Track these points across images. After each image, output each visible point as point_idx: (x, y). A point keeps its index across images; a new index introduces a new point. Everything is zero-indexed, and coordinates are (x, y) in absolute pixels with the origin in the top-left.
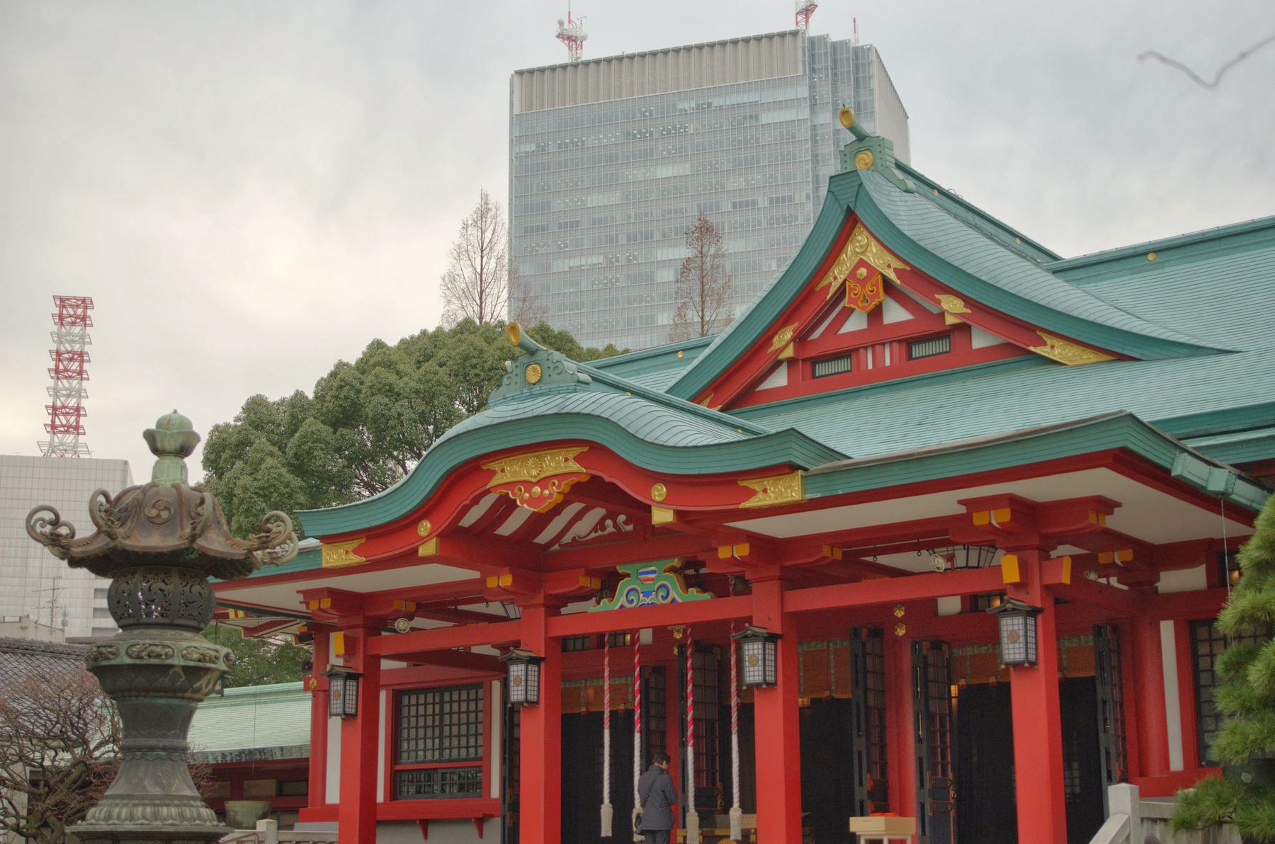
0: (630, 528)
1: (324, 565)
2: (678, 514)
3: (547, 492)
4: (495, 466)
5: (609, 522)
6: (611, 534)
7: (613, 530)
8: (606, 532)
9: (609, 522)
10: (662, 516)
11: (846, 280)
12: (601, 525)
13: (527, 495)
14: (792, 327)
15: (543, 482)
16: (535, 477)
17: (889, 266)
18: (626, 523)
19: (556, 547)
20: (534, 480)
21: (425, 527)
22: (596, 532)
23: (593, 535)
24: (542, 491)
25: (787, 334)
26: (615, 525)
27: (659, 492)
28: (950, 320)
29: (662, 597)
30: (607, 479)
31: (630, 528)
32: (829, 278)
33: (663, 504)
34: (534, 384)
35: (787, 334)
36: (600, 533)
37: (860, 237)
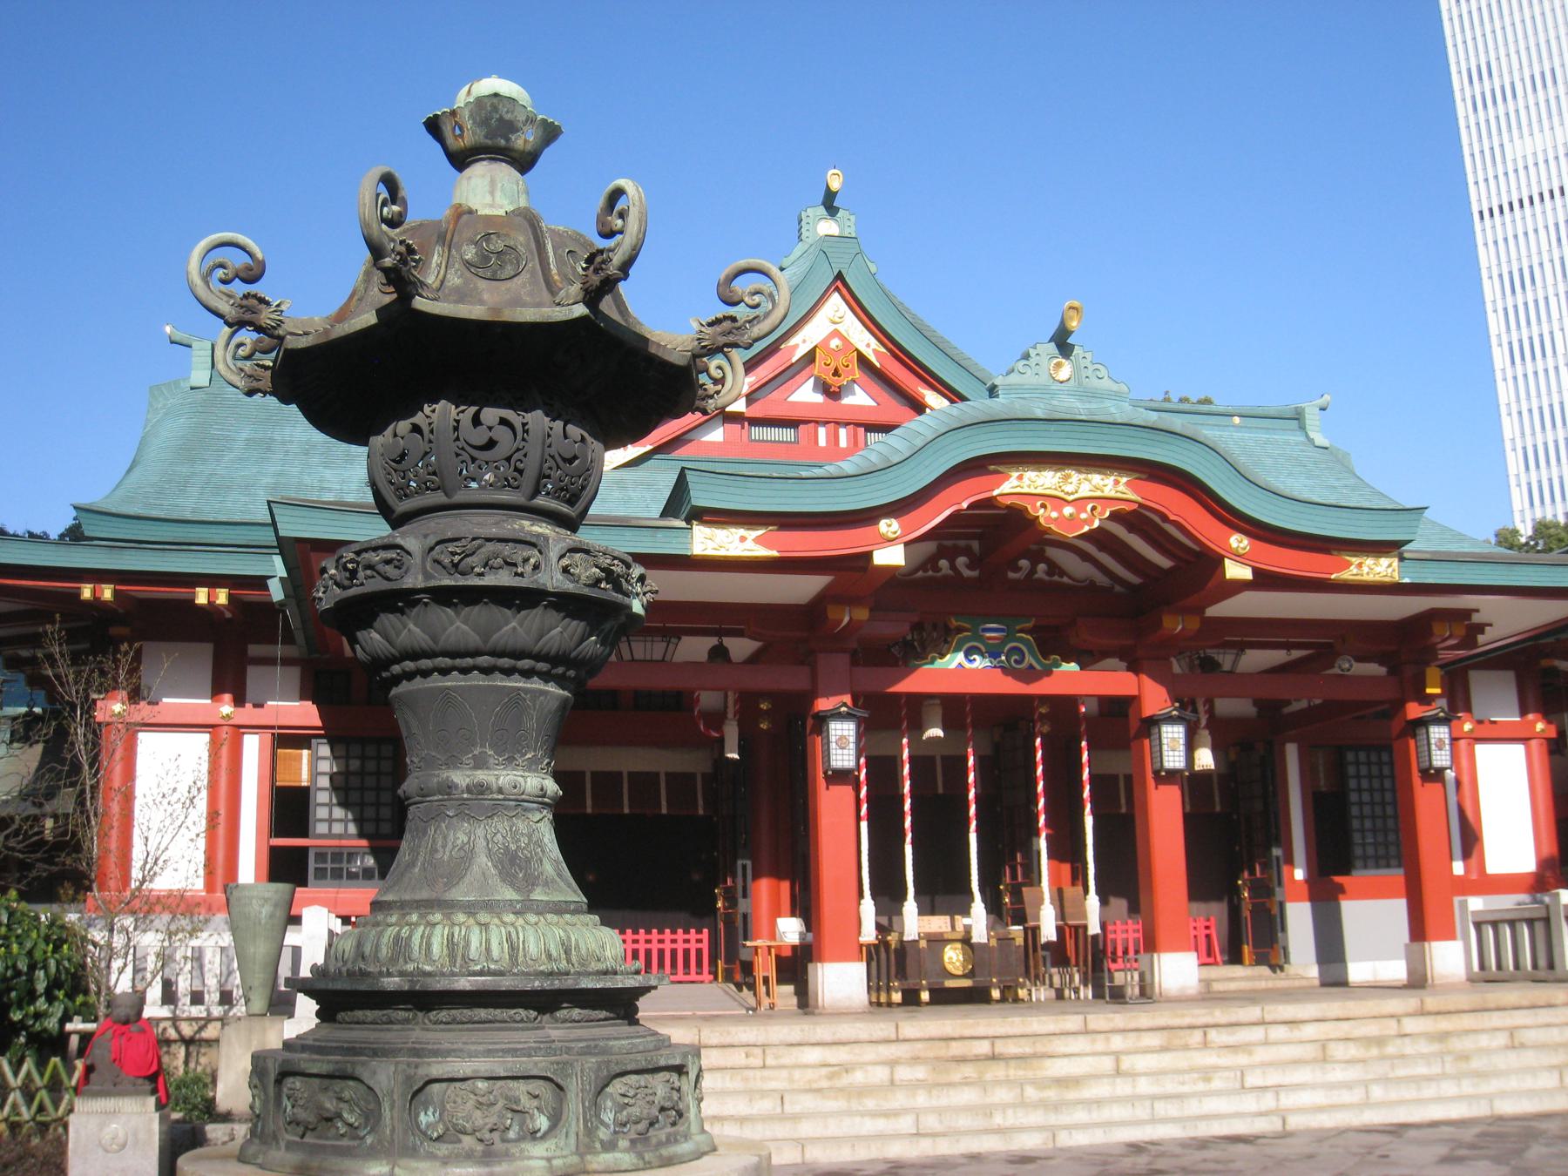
0: (975, 574)
2: (1256, 571)
5: (943, 563)
6: (946, 577)
7: (951, 572)
8: (939, 574)
9: (943, 563)
11: (816, 347)
16: (1072, 493)
17: (868, 346)
21: (889, 526)
22: (926, 571)
23: (920, 574)
26: (953, 567)
27: (1239, 542)
29: (1016, 661)
31: (975, 574)
33: (1239, 558)
34: (1062, 382)
36: (930, 573)
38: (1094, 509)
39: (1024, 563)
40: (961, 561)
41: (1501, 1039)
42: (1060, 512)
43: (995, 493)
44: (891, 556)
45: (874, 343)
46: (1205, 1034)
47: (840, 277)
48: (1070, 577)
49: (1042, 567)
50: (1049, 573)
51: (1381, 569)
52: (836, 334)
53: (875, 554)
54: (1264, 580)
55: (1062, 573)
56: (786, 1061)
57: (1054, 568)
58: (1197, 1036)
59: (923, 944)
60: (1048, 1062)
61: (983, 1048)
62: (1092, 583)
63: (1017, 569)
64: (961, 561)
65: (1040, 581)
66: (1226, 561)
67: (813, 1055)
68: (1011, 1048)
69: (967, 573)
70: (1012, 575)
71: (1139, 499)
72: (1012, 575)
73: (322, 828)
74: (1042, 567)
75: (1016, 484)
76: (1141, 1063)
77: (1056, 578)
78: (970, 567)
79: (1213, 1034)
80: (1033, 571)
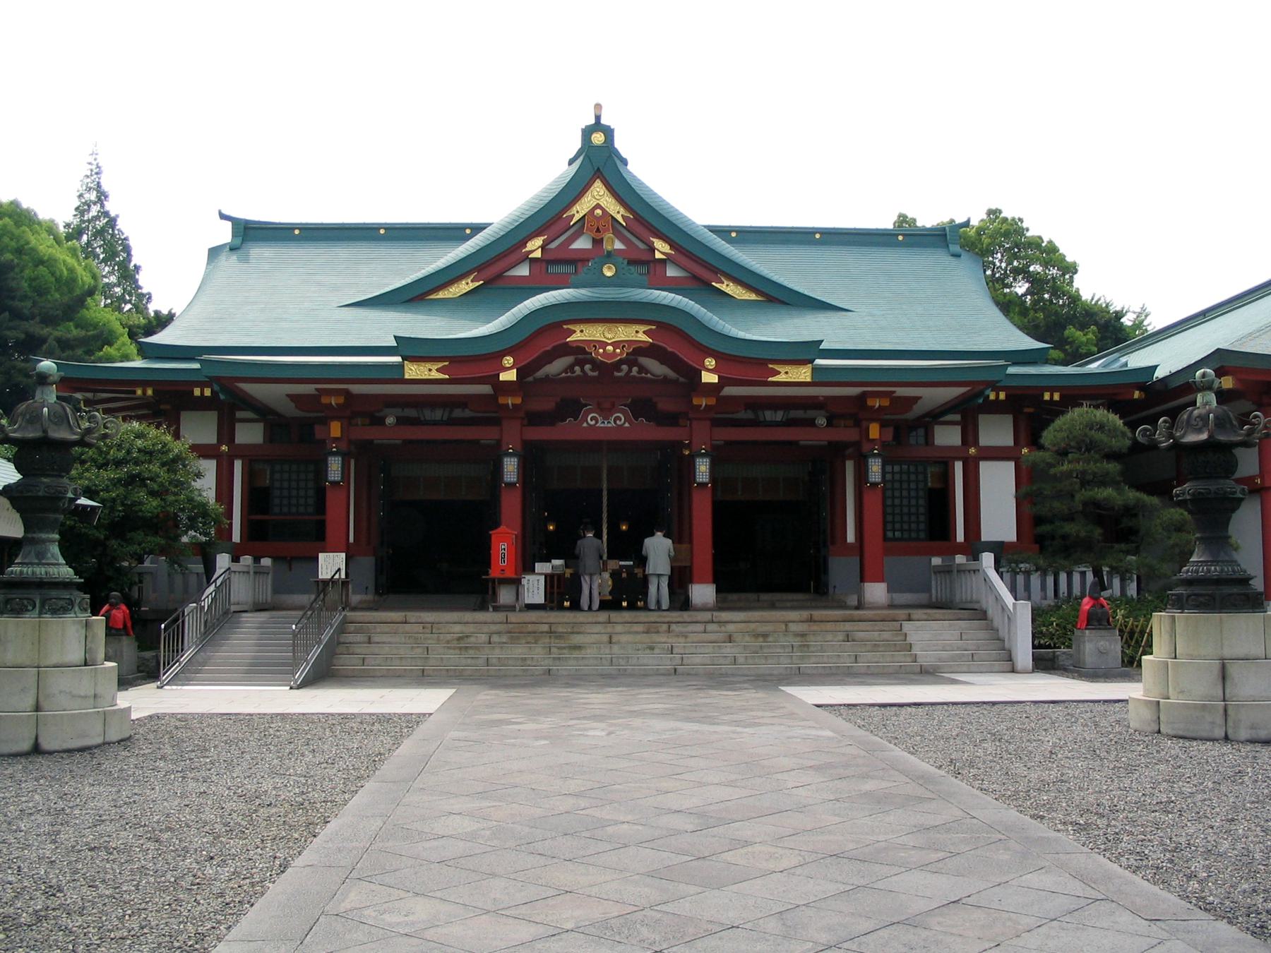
0: (596, 374)
1: (407, 376)
3: (618, 351)
4: (577, 328)
5: (577, 368)
6: (579, 375)
9: (577, 368)
10: (709, 378)
12: (570, 368)
13: (601, 351)
14: (543, 238)
15: (615, 344)
18: (592, 370)
19: (531, 379)
20: (609, 342)
21: (508, 361)
24: (614, 350)
25: (538, 242)
27: (710, 362)
28: (658, 255)
30: (670, 349)
31: (596, 374)
32: (574, 210)
35: (538, 242)
36: (569, 374)
37: (598, 188)
38: (624, 346)
39: (625, 367)
40: (587, 367)
41: (841, 636)
42: (604, 350)
43: (568, 340)
44: (509, 376)
45: (622, 211)
46: (669, 626)
47: (598, 169)
48: (651, 374)
49: (635, 369)
50: (639, 372)
51: (803, 374)
52: (598, 206)
53: (501, 375)
54: (724, 381)
55: (647, 372)
56: (443, 631)
57: (642, 369)
58: (665, 627)
59: (624, 575)
60: (573, 636)
61: (545, 628)
62: (665, 377)
63: (620, 370)
64: (587, 367)
65: (634, 377)
66: (703, 372)
67: (457, 628)
68: (560, 629)
69: (591, 374)
70: (616, 374)
71: (651, 340)
72: (616, 374)
73: (277, 510)
74: (635, 369)
75: (582, 334)
76: (624, 638)
77: (643, 375)
78: (592, 370)
79: (673, 627)
80: (630, 370)
